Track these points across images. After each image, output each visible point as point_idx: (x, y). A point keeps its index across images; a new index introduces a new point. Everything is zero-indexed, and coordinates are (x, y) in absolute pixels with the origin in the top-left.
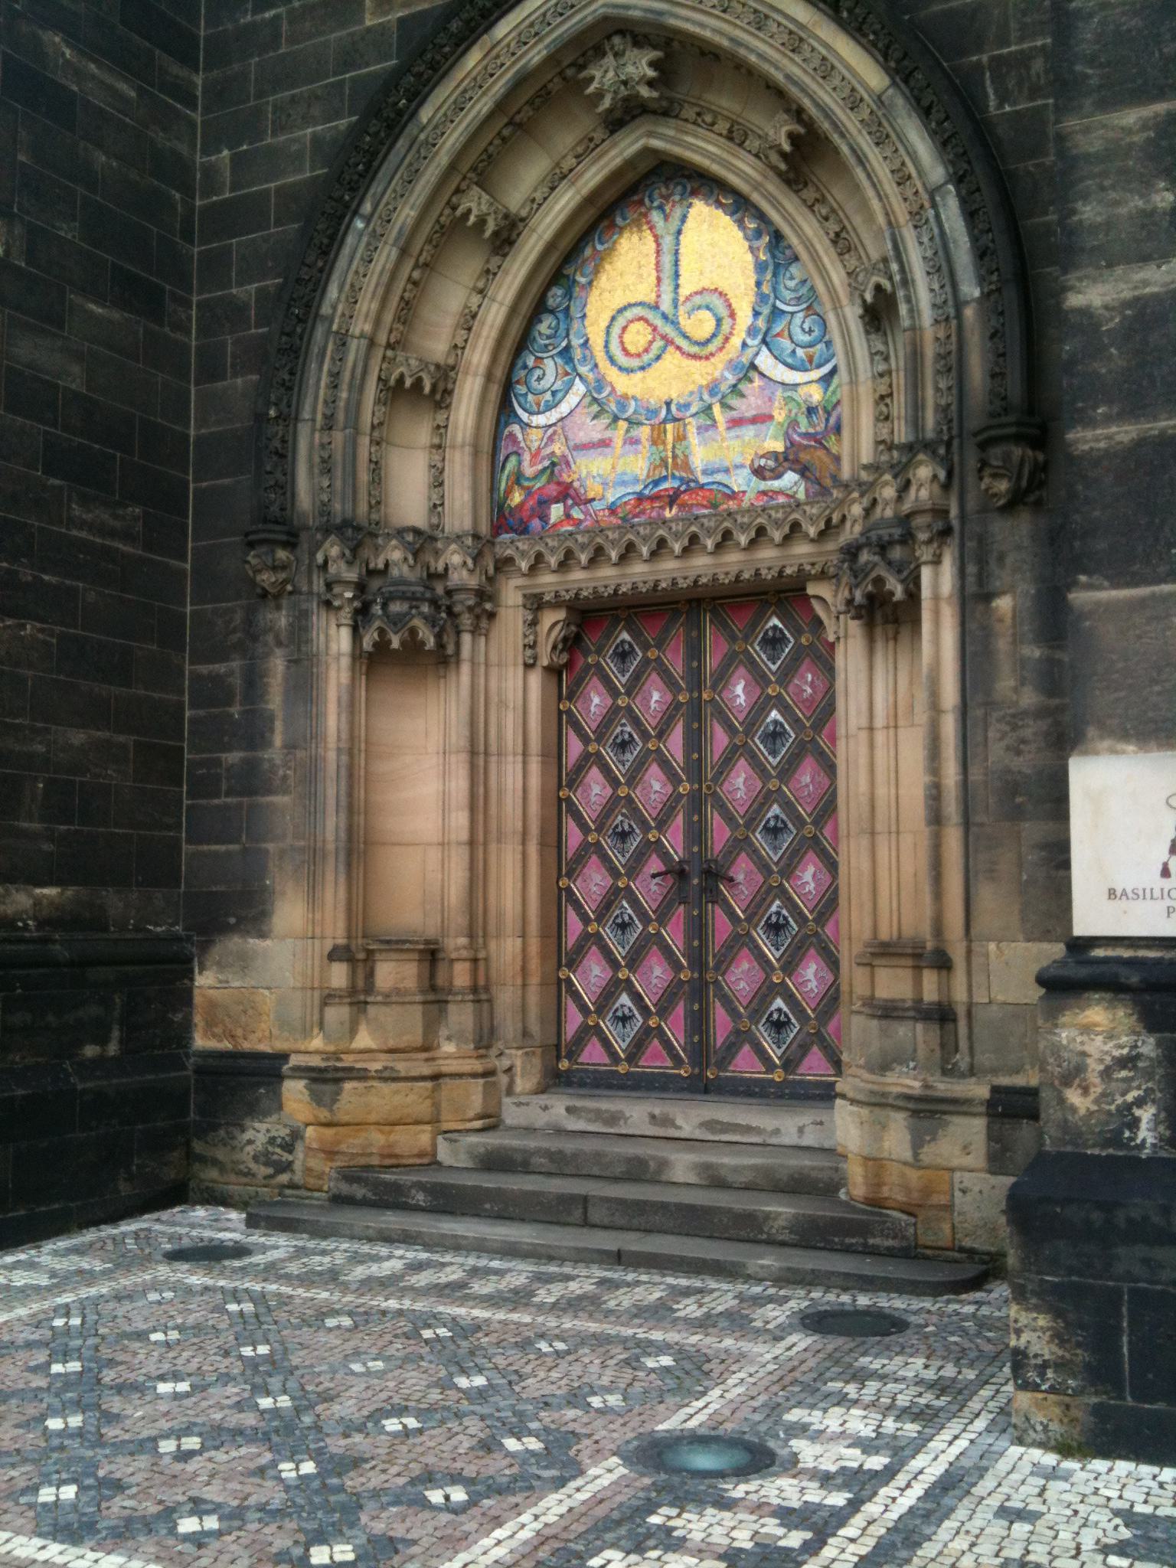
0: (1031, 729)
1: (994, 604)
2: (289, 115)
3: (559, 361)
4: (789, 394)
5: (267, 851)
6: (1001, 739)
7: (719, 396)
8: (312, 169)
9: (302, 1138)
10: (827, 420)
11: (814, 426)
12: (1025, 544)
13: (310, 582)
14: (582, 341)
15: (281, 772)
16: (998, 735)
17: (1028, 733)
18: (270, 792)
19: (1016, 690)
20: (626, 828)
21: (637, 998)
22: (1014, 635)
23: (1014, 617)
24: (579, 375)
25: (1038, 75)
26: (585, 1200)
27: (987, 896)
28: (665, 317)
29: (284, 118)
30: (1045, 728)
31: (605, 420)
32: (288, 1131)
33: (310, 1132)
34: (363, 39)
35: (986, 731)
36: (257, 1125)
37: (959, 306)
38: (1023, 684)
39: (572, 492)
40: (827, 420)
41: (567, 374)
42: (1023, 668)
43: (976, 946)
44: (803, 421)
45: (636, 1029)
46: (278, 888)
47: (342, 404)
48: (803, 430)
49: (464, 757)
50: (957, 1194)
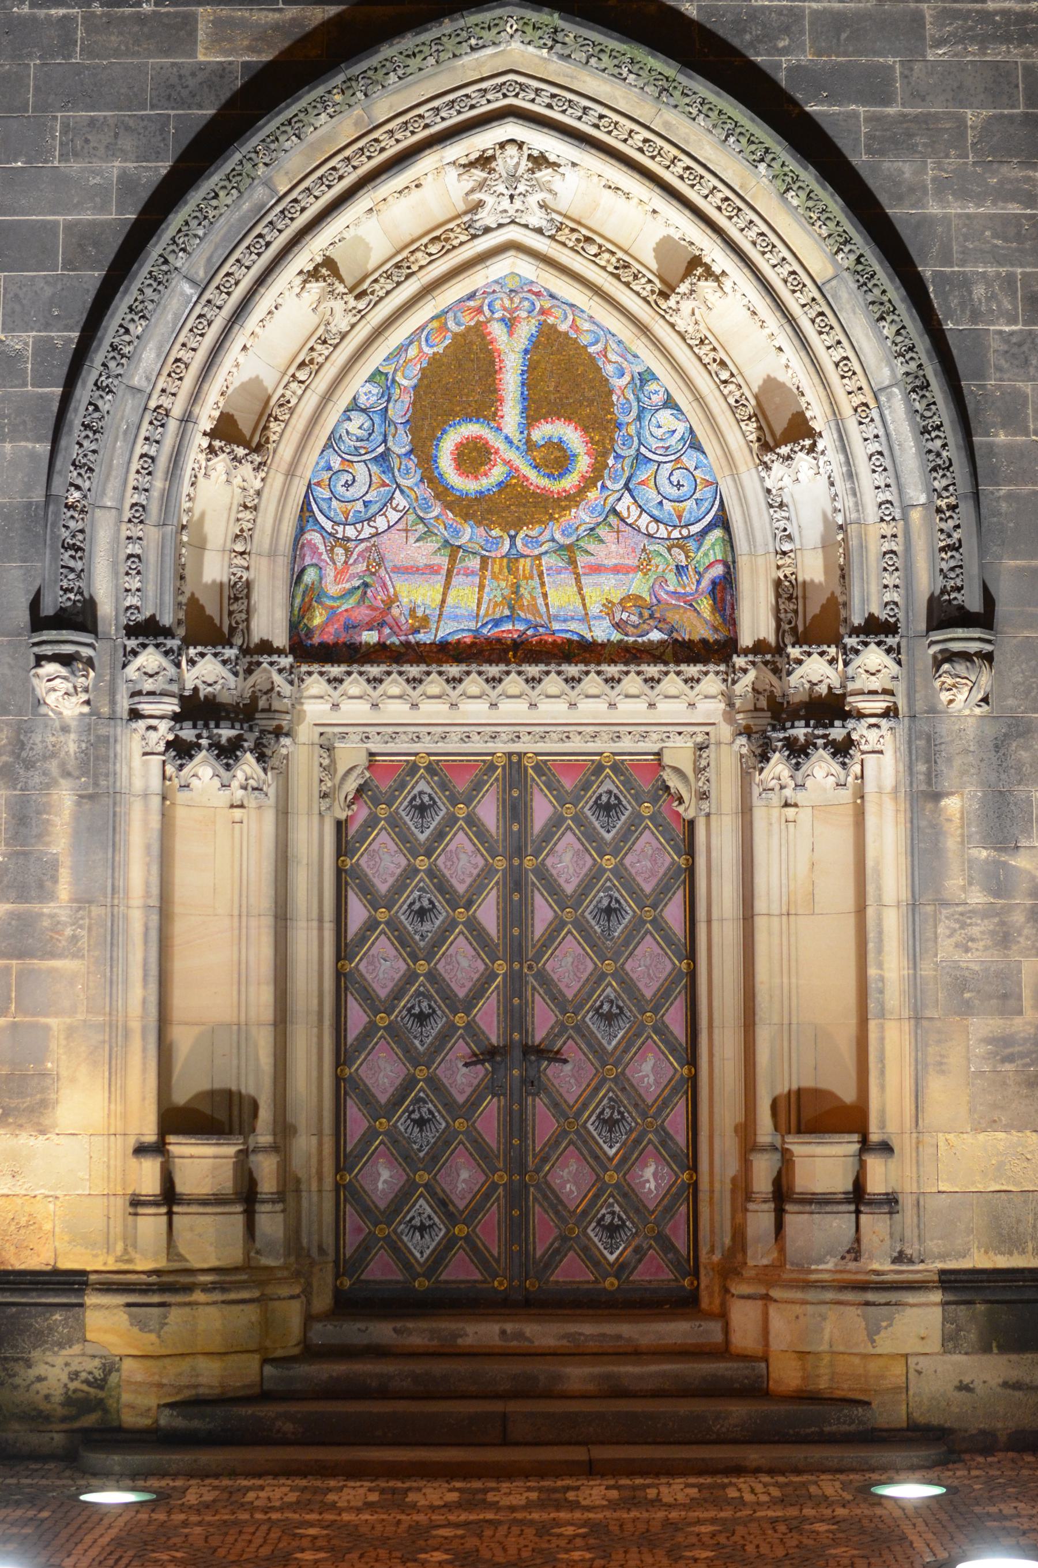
0: (979, 928)
1: (943, 803)
2: (87, 141)
3: (374, 468)
4: (656, 547)
5: (47, 1028)
6: (950, 936)
7: (574, 538)
8: (118, 213)
9: (118, 1370)
10: (699, 582)
11: (684, 586)
12: (972, 749)
13: (113, 702)
14: (403, 451)
15: (68, 932)
16: (948, 932)
17: (975, 931)
18: (52, 955)
19: (963, 889)
20: (427, 1011)
21: (443, 1204)
22: (962, 835)
23: (962, 818)
24: (398, 486)
25: (980, 300)
26: (504, 1416)
27: (936, 1087)
28: (509, 441)
29: (79, 143)
30: (991, 927)
31: (431, 545)
32: (97, 1362)
33: (127, 1365)
34: (193, 74)
35: (936, 927)
36: (50, 1358)
37: (906, 508)
38: (970, 884)
39: (389, 619)
40: (699, 582)
41: (384, 485)
42: (970, 868)
43: (927, 1138)
44: (671, 577)
45: (437, 1239)
46: (64, 1073)
47: (155, 494)
48: (671, 589)
49: (268, 921)
50: (912, 1375)
